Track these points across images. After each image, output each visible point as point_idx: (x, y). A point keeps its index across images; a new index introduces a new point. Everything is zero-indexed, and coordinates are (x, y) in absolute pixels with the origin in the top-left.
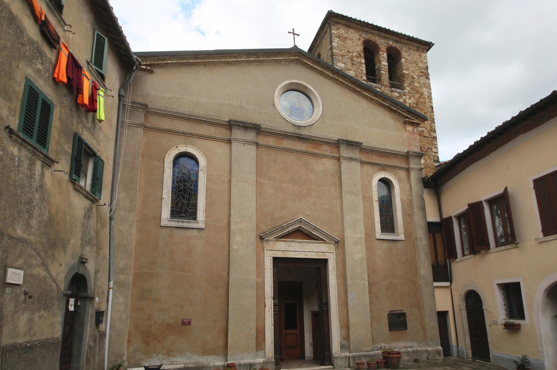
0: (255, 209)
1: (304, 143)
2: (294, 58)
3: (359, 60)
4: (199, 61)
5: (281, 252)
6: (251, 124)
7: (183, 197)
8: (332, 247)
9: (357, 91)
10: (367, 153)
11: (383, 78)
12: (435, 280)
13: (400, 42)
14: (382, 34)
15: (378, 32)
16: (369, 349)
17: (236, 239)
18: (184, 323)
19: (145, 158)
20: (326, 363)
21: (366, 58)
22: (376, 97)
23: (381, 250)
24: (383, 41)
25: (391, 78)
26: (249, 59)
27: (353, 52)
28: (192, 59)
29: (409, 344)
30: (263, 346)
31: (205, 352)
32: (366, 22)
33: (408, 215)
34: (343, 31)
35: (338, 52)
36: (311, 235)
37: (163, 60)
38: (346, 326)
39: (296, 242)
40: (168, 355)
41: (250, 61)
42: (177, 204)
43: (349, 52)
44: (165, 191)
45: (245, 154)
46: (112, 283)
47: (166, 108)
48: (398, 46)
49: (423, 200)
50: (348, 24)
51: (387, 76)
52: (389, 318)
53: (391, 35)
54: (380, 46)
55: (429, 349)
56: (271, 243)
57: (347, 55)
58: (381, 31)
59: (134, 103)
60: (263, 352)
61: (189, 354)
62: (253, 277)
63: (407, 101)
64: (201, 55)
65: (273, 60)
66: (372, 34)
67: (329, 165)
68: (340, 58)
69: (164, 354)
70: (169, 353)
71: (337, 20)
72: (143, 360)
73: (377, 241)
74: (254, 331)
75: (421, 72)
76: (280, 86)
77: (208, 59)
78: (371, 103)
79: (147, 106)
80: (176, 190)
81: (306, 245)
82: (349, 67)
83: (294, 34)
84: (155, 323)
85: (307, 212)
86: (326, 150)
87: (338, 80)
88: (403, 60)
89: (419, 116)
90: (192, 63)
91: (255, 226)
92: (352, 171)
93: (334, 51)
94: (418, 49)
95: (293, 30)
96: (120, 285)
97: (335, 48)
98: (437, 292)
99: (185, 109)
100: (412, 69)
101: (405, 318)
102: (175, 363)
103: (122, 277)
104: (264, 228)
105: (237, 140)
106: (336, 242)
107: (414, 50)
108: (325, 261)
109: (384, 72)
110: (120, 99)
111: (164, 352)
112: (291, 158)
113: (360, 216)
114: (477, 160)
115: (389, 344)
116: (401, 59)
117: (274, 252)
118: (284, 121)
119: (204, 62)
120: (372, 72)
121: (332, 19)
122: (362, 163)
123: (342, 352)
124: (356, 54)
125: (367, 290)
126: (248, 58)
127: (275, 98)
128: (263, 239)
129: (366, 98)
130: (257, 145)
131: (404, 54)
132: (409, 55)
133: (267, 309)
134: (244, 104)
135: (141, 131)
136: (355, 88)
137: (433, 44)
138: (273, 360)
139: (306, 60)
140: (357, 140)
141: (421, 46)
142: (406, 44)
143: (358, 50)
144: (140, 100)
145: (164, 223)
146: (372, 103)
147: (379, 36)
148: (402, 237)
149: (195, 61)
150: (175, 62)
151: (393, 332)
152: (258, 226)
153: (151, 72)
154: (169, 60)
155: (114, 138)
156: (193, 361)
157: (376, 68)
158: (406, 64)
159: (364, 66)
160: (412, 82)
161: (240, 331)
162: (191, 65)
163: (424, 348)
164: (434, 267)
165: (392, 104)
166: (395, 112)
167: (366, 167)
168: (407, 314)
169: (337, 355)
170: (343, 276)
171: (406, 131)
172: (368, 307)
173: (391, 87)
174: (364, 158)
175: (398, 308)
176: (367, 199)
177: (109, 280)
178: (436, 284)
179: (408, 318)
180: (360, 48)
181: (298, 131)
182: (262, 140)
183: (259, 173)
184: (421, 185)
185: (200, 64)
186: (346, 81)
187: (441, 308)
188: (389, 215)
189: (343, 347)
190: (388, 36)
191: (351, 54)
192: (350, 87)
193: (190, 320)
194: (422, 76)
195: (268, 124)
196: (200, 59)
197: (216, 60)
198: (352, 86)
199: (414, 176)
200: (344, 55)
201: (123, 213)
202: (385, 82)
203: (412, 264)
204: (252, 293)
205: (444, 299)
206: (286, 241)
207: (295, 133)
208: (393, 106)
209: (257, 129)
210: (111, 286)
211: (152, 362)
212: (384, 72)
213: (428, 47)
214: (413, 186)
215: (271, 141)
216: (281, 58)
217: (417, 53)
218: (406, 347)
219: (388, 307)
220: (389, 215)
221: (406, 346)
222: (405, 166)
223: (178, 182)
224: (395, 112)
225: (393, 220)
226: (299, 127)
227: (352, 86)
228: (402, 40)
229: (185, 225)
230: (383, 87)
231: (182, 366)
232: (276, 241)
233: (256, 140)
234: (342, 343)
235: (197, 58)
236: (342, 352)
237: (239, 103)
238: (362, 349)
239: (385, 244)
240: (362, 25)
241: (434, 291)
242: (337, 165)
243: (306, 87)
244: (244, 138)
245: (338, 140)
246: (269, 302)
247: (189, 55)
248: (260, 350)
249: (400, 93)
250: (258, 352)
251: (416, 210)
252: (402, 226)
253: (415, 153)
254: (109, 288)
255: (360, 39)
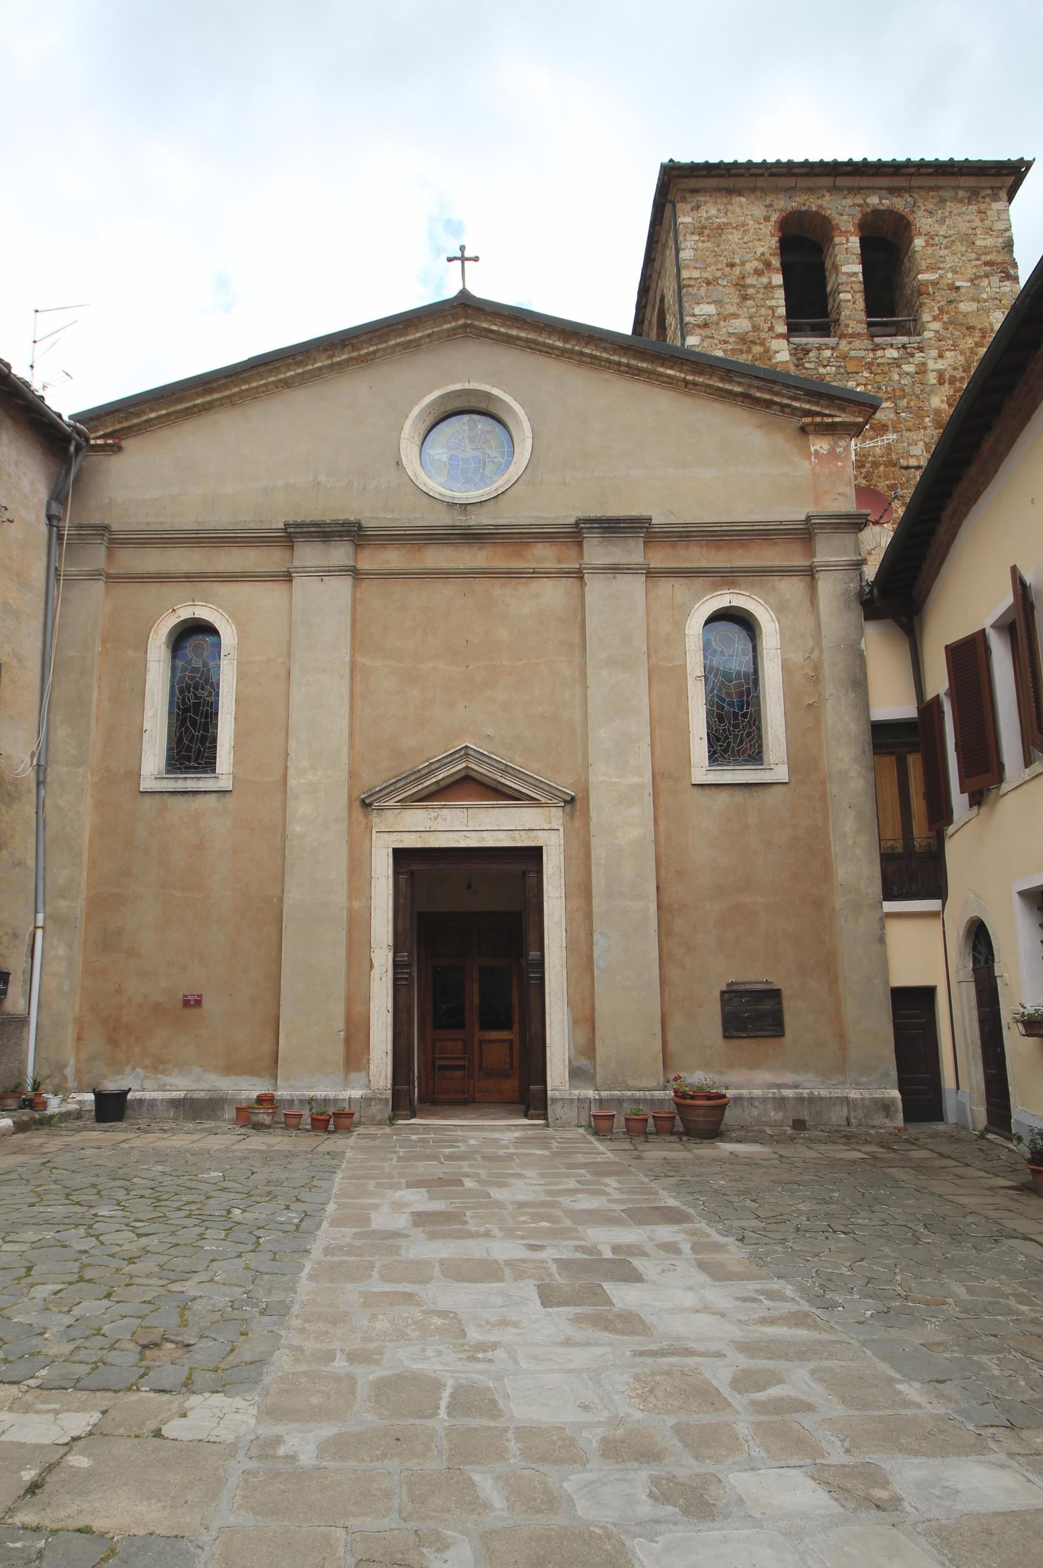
0: (346, 734)
1: (480, 549)
2: (454, 324)
3: (765, 280)
4: (216, 396)
5: (413, 836)
6: (335, 523)
7: (194, 723)
8: (556, 816)
9: (641, 371)
10: (673, 545)
11: (845, 313)
12: (889, 895)
13: (909, 190)
14: (841, 181)
15: (827, 181)
16: (653, 1084)
17: (302, 808)
18: (186, 1003)
19: (108, 646)
20: (531, 1112)
21: (786, 270)
22: (701, 373)
23: (706, 817)
24: (848, 202)
25: (873, 307)
26: (335, 360)
27: (743, 263)
28: (199, 395)
29: (789, 1078)
30: (365, 1061)
31: (231, 1068)
32: (784, 160)
33: (804, 709)
34: (711, 210)
35: (696, 274)
36: (499, 787)
37: (138, 415)
38: (585, 1019)
39: (456, 807)
40: (155, 1069)
41: (339, 363)
42: (180, 740)
43: (732, 265)
44: (148, 713)
45: (323, 601)
46: (40, 916)
47: (148, 524)
48: (899, 204)
49: (860, 659)
50: (730, 183)
51: (861, 304)
52: (724, 1003)
53: (874, 175)
54: (837, 219)
55: (854, 1094)
56: (390, 815)
57: (724, 276)
58: (836, 175)
59: (80, 527)
60: (363, 1074)
61: (197, 1070)
62: (339, 898)
63: (931, 365)
64: (216, 380)
65: (398, 345)
66: (811, 190)
67: (552, 594)
68: (703, 291)
69: (146, 1068)
70: (158, 1065)
71: (693, 183)
72: (105, 1077)
73: (699, 791)
74: (340, 1024)
75: (986, 264)
76: (416, 410)
77: (235, 386)
78: (686, 395)
79: (106, 528)
80: (179, 708)
81: (482, 814)
82: (732, 309)
83: (463, 259)
84: (130, 1000)
85: (486, 731)
86: (544, 556)
87: (582, 354)
88: (919, 242)
89: (849, 401)
90: (202, 405)
91: (346, 774)
92: (617, 602)
93: (685, 274)
94: (974, 194)
95: (462, 248)
96: (57, 920)
97: (687, 267)
98: (896, 931)
99: (186, 521)
100: (950, 261)
101: (780, 1003)
102: (168, 1087)
103: (63, 903)
104: (372, 779)
105: (307, 572)
106: (565, 801)
107: (961, 201)
108: (535, 854)
109: (849, 296)
110: (51, 525)
111: (148, 1062)
112: (446, 592)
113: (640, 726)
114: (973, 498)
115: (721, 1073)
116: (911, 241)
117: (395, 836)
118: (426, 500)
119: (228, 397)
120: (808, 304)
121: (678, 183)
122: (651, 574)
123: (572, 1086)
124: (755, 264)
125: (654, 924)
126: (330, 357)
127: (402, 446)
128: (370, 805)
129: (670, 383)
130: (356, 574)
131: (923, 222)
132: (942, 222)
133: (376, 973)
134: (322, 478)
135: (98, 587)
136: (633, 362)
137: (1028, 165)
138: (389, 1094)
139: (486, 320)
140: (635, 513)
141: (985, 182)
142: (931, 189)
143: (760, 250)
144: (96, 519)
145: (147, 784)
146: (693, 396)
147: (834, 189)
148: (781, 773)
149: (208, 398)
150: (164, 412)
151: (735, 1043)
152: (353, 775)
153: (117, 449)
154: (152, 411)
155: (42, 612)
156: (206, 1086)
157: (829, 289)
158: (929, 250)
159: (780, 294)
160: (950, 302)
161: (309, 1023)
162: (200, 411)
163: (838, 1093)
164: (887, 858)
165: (755, 383)
166: (769, 404)
167: (666, 587)
168: (786, 993)
169: (557, 1095)
170: (582, 890)
171: (808, 455)
172: (656, 971)
173: (872, 336)
174: (659, 559)
175: (755, 974)
176: (664, 675)
177: (36, 912)
178: (890, 906)
179: (789, 1007)
180: (768, 244)
181: (460, 520)
182: (368, 561)
183: (358, 641)
184: (857, 611)
185: (221, 403)
186: (605, 350)
187: (904, 977)
188: (745, 716)
189: (576, 1074)
190: (865, 182)
191: (737, 271)
192: (619, 364)
193: (200, 996)
194: (987, 276)
195: (382, 515)
196: (218, 390)
197: (254, 385)
198: (624, 360)
199: (831, 589)
200: (716, 279)
201: (65, 769)
202: (852, 324)
203: (813, 852)
204: (340, 935)
205: (919, 950)
206: (426, 808)
207: (453, 527)
208: (759, 389)
209: (354, 533)
210: (40, 923)
211: (124, 1082)
212: (849, 296)
213: (1010, 180)
214: (824, 618)
215: (393, 558)
216: (418, 335)
217: (973, 208)
218: (779, 1086)
219: (721, 971)
220: (745, 716)
221: (779, 1081)
222: (799, 561)
223: (182, 691)
224: (769, 404)
225: (759, 729)
226: (465, 507)
227: (624, 360)
228: (916, 182)
229: (191, 785)
230: (843, 343)
231: (182, 1094)
232: (404, 808)
233: (352, 563)
234: (575, 1064)
235: (211, 391)
236: (572, 1086)
237: (311, 478)
238: (631, 1082)
239: (723, 798)
240: (772, 175)
241: (883, 928)
242: (576, 591)
243: (488, 396)
244: (325, 563)
245: (577, 524)
246: (383, 958)
247: (190, 388)
248: (358, 1069)
249: (904, 347)
250: (353, 1075)
251: (830, 689)
252: (783, 741)
253: (830, 517)
254: (36, 928)
255: (767, 219)
